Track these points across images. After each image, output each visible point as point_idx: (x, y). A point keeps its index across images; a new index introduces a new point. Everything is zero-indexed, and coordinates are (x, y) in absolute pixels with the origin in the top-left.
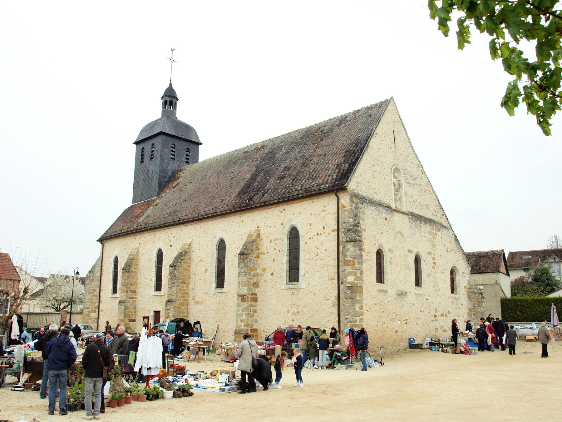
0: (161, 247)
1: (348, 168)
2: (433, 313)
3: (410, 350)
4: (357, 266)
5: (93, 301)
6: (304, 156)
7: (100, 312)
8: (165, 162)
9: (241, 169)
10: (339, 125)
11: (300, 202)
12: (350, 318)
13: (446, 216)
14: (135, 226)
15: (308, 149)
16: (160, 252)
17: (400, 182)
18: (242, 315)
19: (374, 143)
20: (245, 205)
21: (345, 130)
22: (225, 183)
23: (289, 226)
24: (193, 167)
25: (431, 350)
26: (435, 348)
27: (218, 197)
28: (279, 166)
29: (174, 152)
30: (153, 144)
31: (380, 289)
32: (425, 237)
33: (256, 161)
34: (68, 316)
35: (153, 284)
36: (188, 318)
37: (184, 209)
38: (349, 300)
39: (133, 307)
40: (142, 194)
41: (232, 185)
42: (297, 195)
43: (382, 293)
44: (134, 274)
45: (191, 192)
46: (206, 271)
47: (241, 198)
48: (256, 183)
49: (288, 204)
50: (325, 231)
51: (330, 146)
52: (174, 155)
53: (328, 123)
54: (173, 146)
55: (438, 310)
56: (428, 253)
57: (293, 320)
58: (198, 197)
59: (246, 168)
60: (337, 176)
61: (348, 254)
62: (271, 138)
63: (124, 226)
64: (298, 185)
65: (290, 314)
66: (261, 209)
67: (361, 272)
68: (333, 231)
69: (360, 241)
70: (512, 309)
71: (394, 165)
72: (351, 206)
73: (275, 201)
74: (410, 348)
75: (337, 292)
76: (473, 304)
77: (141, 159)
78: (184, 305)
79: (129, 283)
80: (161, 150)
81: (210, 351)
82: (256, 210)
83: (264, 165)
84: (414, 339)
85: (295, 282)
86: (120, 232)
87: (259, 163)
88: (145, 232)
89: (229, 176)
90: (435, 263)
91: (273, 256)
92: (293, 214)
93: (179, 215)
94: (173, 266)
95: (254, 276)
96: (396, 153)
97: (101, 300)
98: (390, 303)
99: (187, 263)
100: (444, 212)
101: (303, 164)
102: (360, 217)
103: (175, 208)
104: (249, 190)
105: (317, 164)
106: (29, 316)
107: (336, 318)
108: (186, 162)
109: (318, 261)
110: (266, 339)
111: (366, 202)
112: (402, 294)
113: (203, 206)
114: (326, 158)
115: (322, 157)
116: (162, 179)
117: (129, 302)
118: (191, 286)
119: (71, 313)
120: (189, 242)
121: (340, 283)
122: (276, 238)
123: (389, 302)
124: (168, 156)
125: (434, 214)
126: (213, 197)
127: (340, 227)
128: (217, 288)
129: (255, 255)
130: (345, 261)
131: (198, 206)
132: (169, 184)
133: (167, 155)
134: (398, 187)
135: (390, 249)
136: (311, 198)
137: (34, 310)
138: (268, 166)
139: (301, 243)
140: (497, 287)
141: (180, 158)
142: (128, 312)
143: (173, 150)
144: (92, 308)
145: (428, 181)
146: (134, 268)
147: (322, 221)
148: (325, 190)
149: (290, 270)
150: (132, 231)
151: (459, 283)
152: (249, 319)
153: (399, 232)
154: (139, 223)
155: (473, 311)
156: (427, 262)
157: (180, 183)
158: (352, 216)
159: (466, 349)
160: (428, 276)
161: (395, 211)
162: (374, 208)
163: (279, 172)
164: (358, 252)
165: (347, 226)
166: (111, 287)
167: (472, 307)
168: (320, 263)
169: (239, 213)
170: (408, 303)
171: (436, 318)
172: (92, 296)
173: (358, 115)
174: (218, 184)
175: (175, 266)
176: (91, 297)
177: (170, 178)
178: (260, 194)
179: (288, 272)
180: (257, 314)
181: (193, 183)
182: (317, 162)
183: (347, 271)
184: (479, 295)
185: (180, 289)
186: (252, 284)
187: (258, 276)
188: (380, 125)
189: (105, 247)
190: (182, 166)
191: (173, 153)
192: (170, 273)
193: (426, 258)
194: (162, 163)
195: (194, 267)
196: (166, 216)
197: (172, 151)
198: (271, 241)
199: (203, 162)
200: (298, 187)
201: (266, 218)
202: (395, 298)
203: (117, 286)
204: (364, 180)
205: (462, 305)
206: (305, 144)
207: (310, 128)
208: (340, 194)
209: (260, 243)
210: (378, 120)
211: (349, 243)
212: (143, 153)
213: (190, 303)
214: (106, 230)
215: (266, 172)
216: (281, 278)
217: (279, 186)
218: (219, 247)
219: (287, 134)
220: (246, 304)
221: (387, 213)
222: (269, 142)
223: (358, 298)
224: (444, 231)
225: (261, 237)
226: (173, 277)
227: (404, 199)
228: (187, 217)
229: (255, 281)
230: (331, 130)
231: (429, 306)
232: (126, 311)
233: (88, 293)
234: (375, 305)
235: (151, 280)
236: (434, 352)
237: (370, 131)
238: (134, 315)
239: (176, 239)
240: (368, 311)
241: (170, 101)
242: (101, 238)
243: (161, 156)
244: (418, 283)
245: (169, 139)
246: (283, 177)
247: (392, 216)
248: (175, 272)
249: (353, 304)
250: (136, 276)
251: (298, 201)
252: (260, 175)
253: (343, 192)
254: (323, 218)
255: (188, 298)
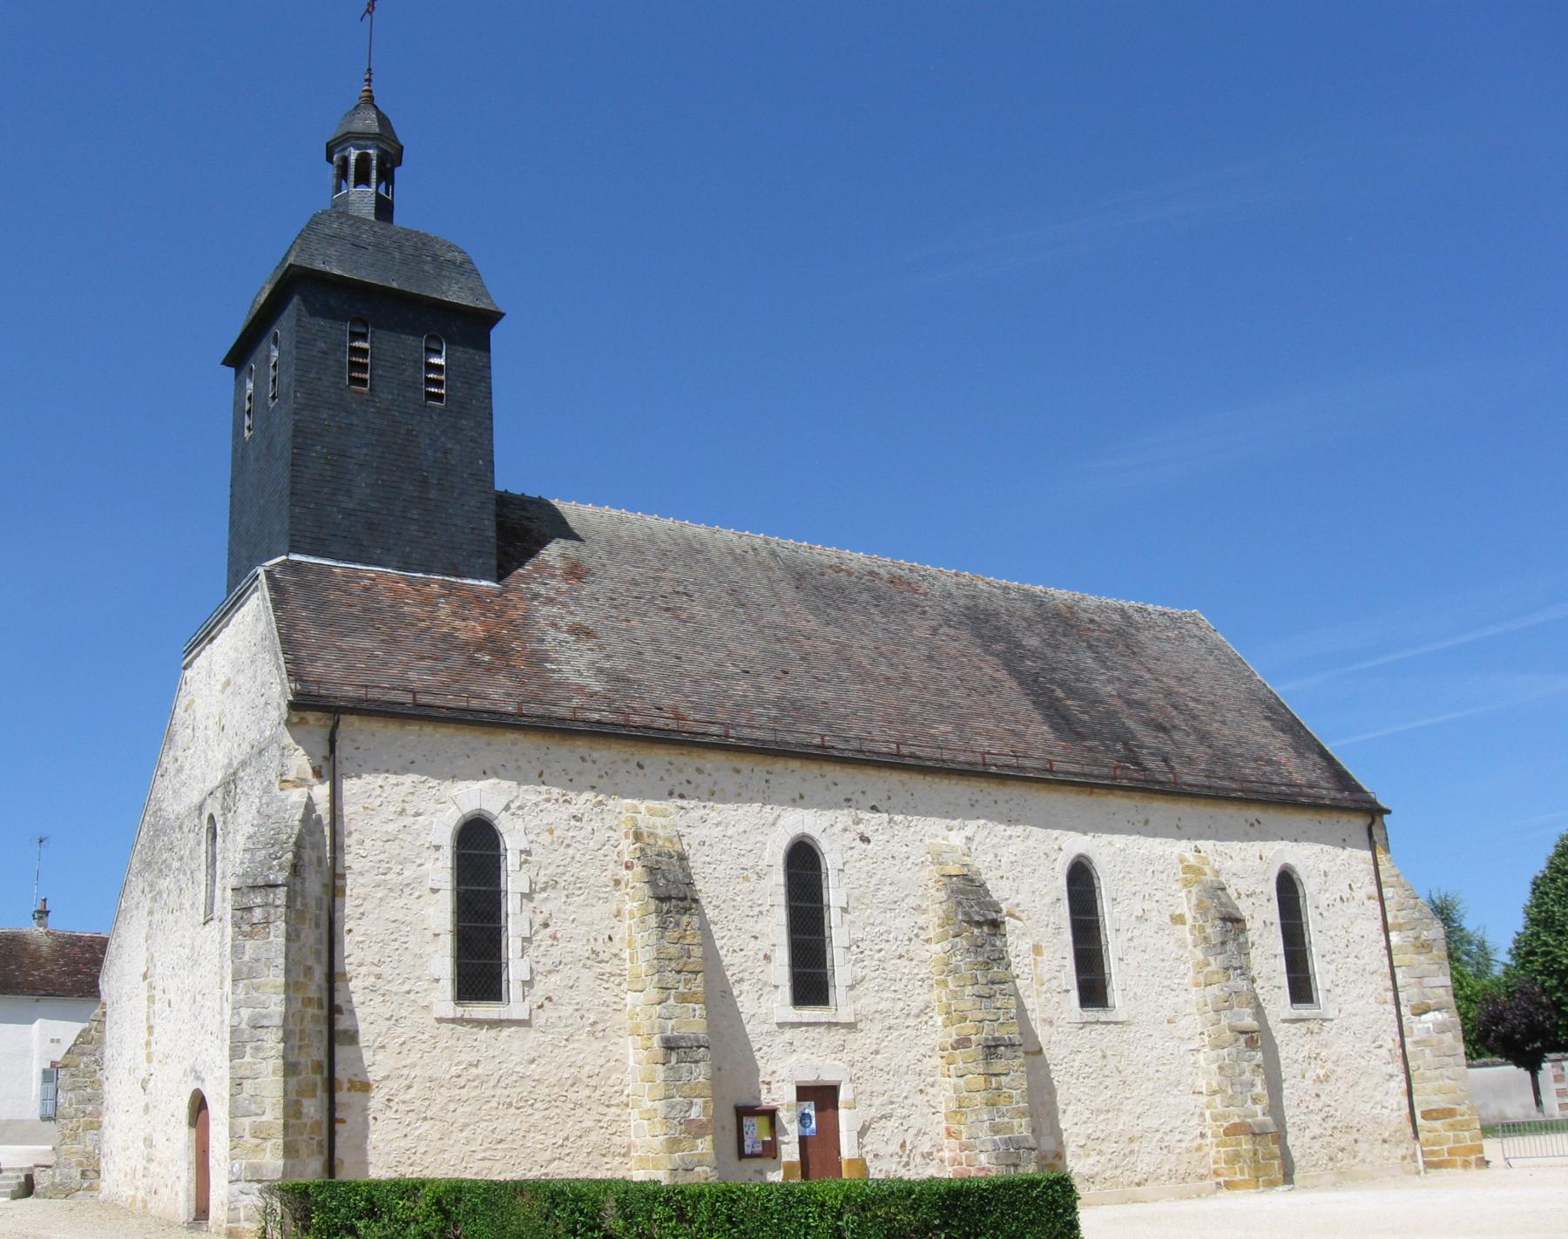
65: (1308, 1082)
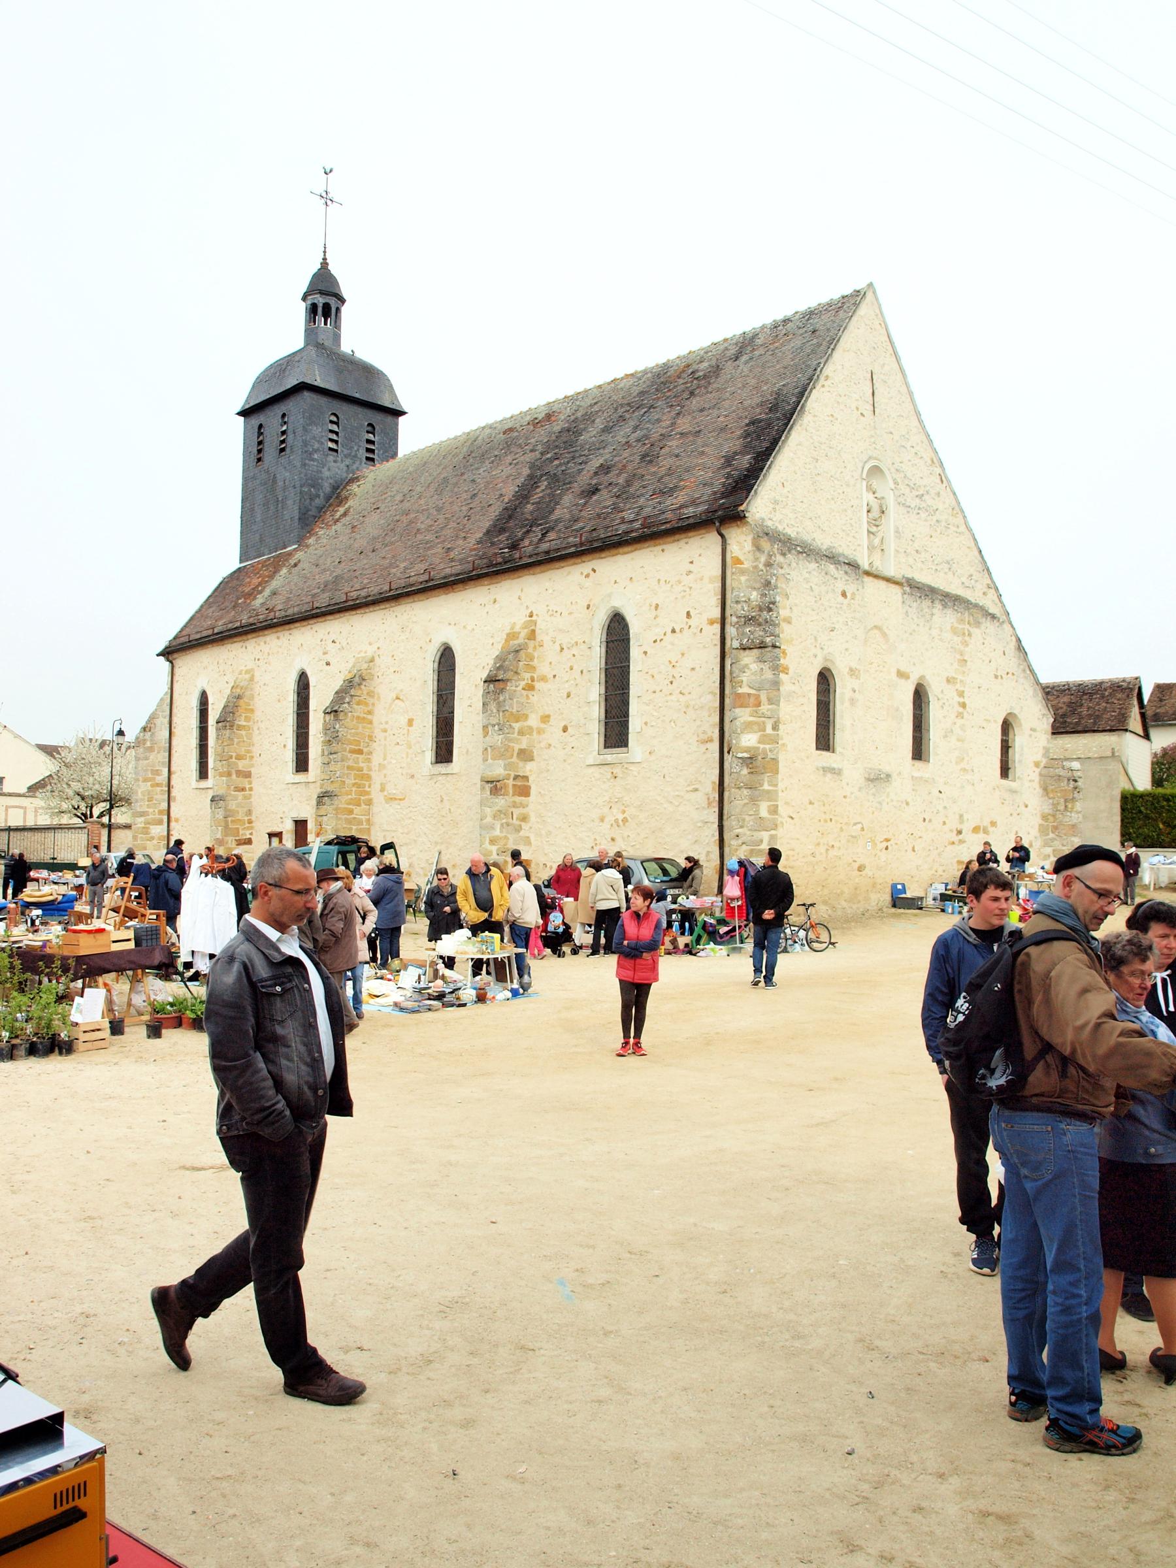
0: (305, 668)
1: (750, 463)
2: (954, 824)
3: (893, 910)
4: (765, 708)
5: (155, 797)
6: (646, 437)
7: (173, 824)
8: (313, 460)
9: (494, 473)
10: (737, 359)
11: (632, 551)
12: (745, 834)
13: (997, 589)
14: (245, 619)
15: (657, 420)
16: (303, 678)
17: (883, 501)
18: (492, 828)
19: (817, 403)
20: (500, 560)
21: (751, 371)
22: (455, 508)
23: (605, 611)
24: (383, 470)
25: (943, 911)
26: (953, 909)
27: (438, 543)
28: (586, 463)
29: (337, 433)
30: (284, 415)
31: (825, 765)
32: (941, 640)
33: (532, 451)
34: (105, 832)
35: (289, 755)
36: (369, 834)
37: (357, 573)
38: (745, 792)
39: (245, 810)
40: (261, 540)
41: (472, 511)
42: (627, 533)
43: (829, 775)
44: (243, 733)
45: (376, 533)
46: (410, 722)
47: (493, 544)
48: (529, 506)
49: (603, 555)
50: (691, 622)
51: (710, 411)
52: (336, 442)
53: (710, 354)
54: (334, 419)
55: (965, 817)
56: (948, 681)
57: (613, 839)
58: (392, 543)
59: (508, 470)
60: (724, 485)
61: (745, 678)
62: (569, 394)
63: (221, 618)
64: (629, 509)
65: (606, 826)
66: (538, 569)
67: (775, 722)
68: (711, 622)
69: (774, 646)
70: (1147, 817)
71: (870, 458)
72: (757, 559)
73: (573, 550)
74: (894, 906)
75: (717, 772)
76: (1053, 804)
77: (256, 452)
78: (359, 805)
79: (234, 755)
80: (305, 430)
81: (420, 911)
82: (526, 572)
83: (551, 460)
84: (903, 885)
85: (618, 747)
86: (210, 632)
87: (539, 456)
88: (266, 632)
89: (466, 492)
90: (964, 705)
91: (566, 685)
92: (616, 582)
93: (346, 589)
94: (333, 712)
95: (521, 733)
96: (875, 428)
97: (172, 794)
98: (848, 800)
99: (366, 704)
100: (991, 579)
101: (644, 457)
102: (776, 587)
103: (338, 572)
104: (512, 524)
105: (677, 456)
106: (11, 833)
107: (713, 835)
108: (368, 459)
109: (673, 697)
110: (546, 883)
111: (793, 551)
112: (877, 779)
113: (402, 565)
114: (699, 441)
115: (691, 438)
116: (308, 501)
117: (236, 798)
118: (376, 759)
119: (110, 827)
120: (369, 654)
121: (726, 750)
122: (573, 642)
123: (845, 797)
124: (322, 443)
125: (967, 585)
126: (426, 543)
127: (728, 612)
128: (437, 762)
129: (522, 684)
130: (739, 696)
131: (391, 565)
132: (326, 511)
133: (318, 441)
134: (877, 515)
135: (851, 670)
136: (657, 541)
137: (25, 821)
138: (561, 465)
139: (635, 652)
140: (1113, 766)
141: (351, 448)
142: (232, 821)
143: (335, 428)
144: (153, 814)
145: (954, 503)
146: (243, 718)
147: (684, 596)
148: (691, 521)
149: (606, 717)
150: (236, 628)
151: (1021, 755)
152: (509, 836)
153: (876, 627)
154: (254, 610)
155: (1052, 824)
156: (945, 701)
157: (351, 510)
158: (758, 585)
159: (1025, 909)
160: (946, 736)
161: (867, 573)
162: (814, 565)
163: (585, 478)
164: (769, 675)
165: (742, 610)
166: (194, 764)
167: (1051, 812)
168: (678, 701)
169: (486, 581)
170: (892, 801)
171: (961, 837)
172: (152, 786)
173: (784, 332)
174: (439, 509)
175: (336, 711)
176: (150, 788)
177: (328, 498)
178: (537, 531)
179: (603, 724)
180: (529, 825)
181: (381, 509)
182: (677, 452)
183: (742, 720)
184: (1068, 784)
185: (349, 768)
186: (515, 754)
187: (531, 734)
188: (837, 355)
189: (176, 670)
190: (358, 469)
191: (334, 437)
192: (326, 729)
193: (942, 691)
194: (307, 461)
195: (380, 715)
196: (315, 591)
197: (331, 431)
198: (562, 649)
199: (407, 458)
200: (629, 515)
201: (550, 591)
202: (860, 789)
203: (207, 762)
204: (790, 496)
205: (1026, 806)
206: (652, 407)
207: (666, 367)
208: (731, 529)
209: (536, 655)
210: (833, 342)
211: (747, 651)
212: (261, 438)
213: (375, 801)
214: (179, 629)
215: (554, 479)
216: (586, 737)
217: (583, 514)
218: (439, 663)
219: (609, 384)
220: (501, 802)
221: (847, 578)
222: (565, 404)
223: (766, 787)
224: (988, 626)
225: (539, 637)
226: (332, 738)
227: (893, 547)
228: (363, 593)
229: (524, 746)
230: (716, 370)
231: (945, 807)
232: (230, 819)
233: (141, 779)
234: (811, 803)
235: (285, 746)
236: (950, 916)
237: (810, 371)
238: (248, 828)
239: (339, 646)
240: (792, 818)
241: (324, 304)
242: (166, 648)
243: (305, 444)
244: (919, 752)
245: (323, 401)
246: (595, 490)
247: (860, 588)
248: (337, 726)
249: (754, 800)
250: (250, 737)
251: (626, 549)
252: (538, 487)
253: (737, 526)
254: (688, 590)
255: (369, 787)
